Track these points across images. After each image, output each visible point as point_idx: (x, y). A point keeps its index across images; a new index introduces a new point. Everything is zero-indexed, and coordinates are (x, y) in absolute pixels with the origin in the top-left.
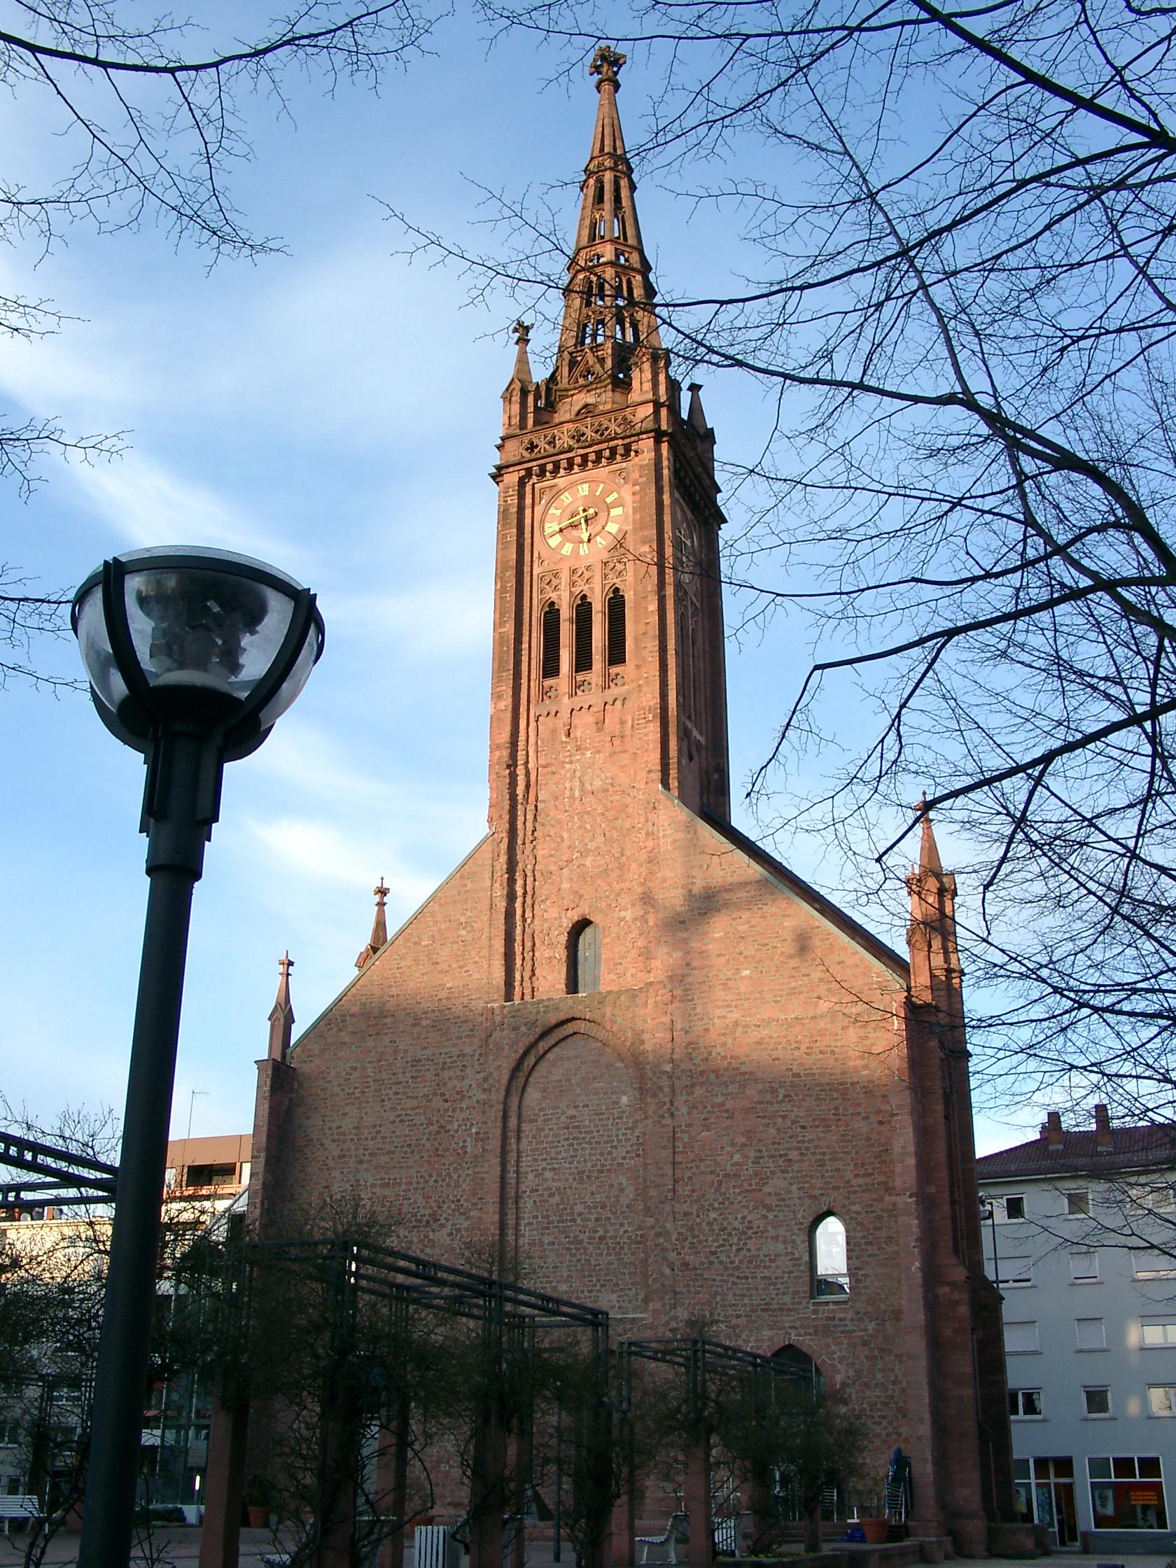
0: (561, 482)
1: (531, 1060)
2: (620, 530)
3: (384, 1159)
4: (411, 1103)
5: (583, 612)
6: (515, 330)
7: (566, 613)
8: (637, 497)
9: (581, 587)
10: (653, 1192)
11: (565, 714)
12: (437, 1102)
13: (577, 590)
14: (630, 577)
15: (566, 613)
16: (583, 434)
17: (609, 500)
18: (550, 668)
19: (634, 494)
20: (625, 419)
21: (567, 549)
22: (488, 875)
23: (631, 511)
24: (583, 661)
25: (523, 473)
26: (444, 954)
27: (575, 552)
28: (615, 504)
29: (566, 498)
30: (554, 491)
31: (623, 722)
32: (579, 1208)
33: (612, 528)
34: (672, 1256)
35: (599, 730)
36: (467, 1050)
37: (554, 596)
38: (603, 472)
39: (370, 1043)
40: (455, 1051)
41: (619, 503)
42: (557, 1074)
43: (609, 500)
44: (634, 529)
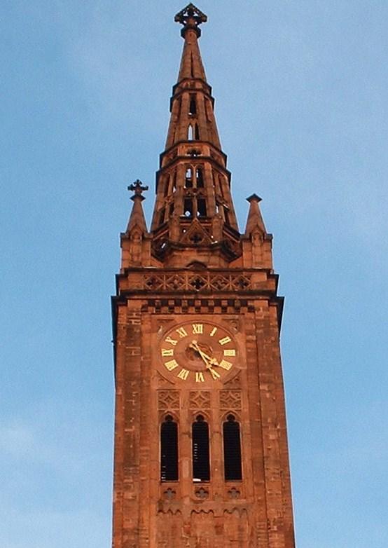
0: (178, 318)
2: (233, 369)
5: (200, 431)
6: (131, 188)
7: (185, 427)
8: (252, 345)
9: (200, 409)
11: (186, 513)
13: (196, 410)
14: (245, 407)
15: (185, 427)
16: (203, 284)
17: (223, 342)
18: (170, 470)
19: (248, 341)
20: (241, 280)
23: (244, 355)
24: (201, 469)
25: (146, 302)
27: (191, 379)
28: (227, 347)
29: (182, 332)
30: (171, 323)
31: (241, 530)
33: (226, 365)
35: (218, 533)
37: (172, 410)
38: (218, 319)
43: (223, 342)
44: (248, 372)
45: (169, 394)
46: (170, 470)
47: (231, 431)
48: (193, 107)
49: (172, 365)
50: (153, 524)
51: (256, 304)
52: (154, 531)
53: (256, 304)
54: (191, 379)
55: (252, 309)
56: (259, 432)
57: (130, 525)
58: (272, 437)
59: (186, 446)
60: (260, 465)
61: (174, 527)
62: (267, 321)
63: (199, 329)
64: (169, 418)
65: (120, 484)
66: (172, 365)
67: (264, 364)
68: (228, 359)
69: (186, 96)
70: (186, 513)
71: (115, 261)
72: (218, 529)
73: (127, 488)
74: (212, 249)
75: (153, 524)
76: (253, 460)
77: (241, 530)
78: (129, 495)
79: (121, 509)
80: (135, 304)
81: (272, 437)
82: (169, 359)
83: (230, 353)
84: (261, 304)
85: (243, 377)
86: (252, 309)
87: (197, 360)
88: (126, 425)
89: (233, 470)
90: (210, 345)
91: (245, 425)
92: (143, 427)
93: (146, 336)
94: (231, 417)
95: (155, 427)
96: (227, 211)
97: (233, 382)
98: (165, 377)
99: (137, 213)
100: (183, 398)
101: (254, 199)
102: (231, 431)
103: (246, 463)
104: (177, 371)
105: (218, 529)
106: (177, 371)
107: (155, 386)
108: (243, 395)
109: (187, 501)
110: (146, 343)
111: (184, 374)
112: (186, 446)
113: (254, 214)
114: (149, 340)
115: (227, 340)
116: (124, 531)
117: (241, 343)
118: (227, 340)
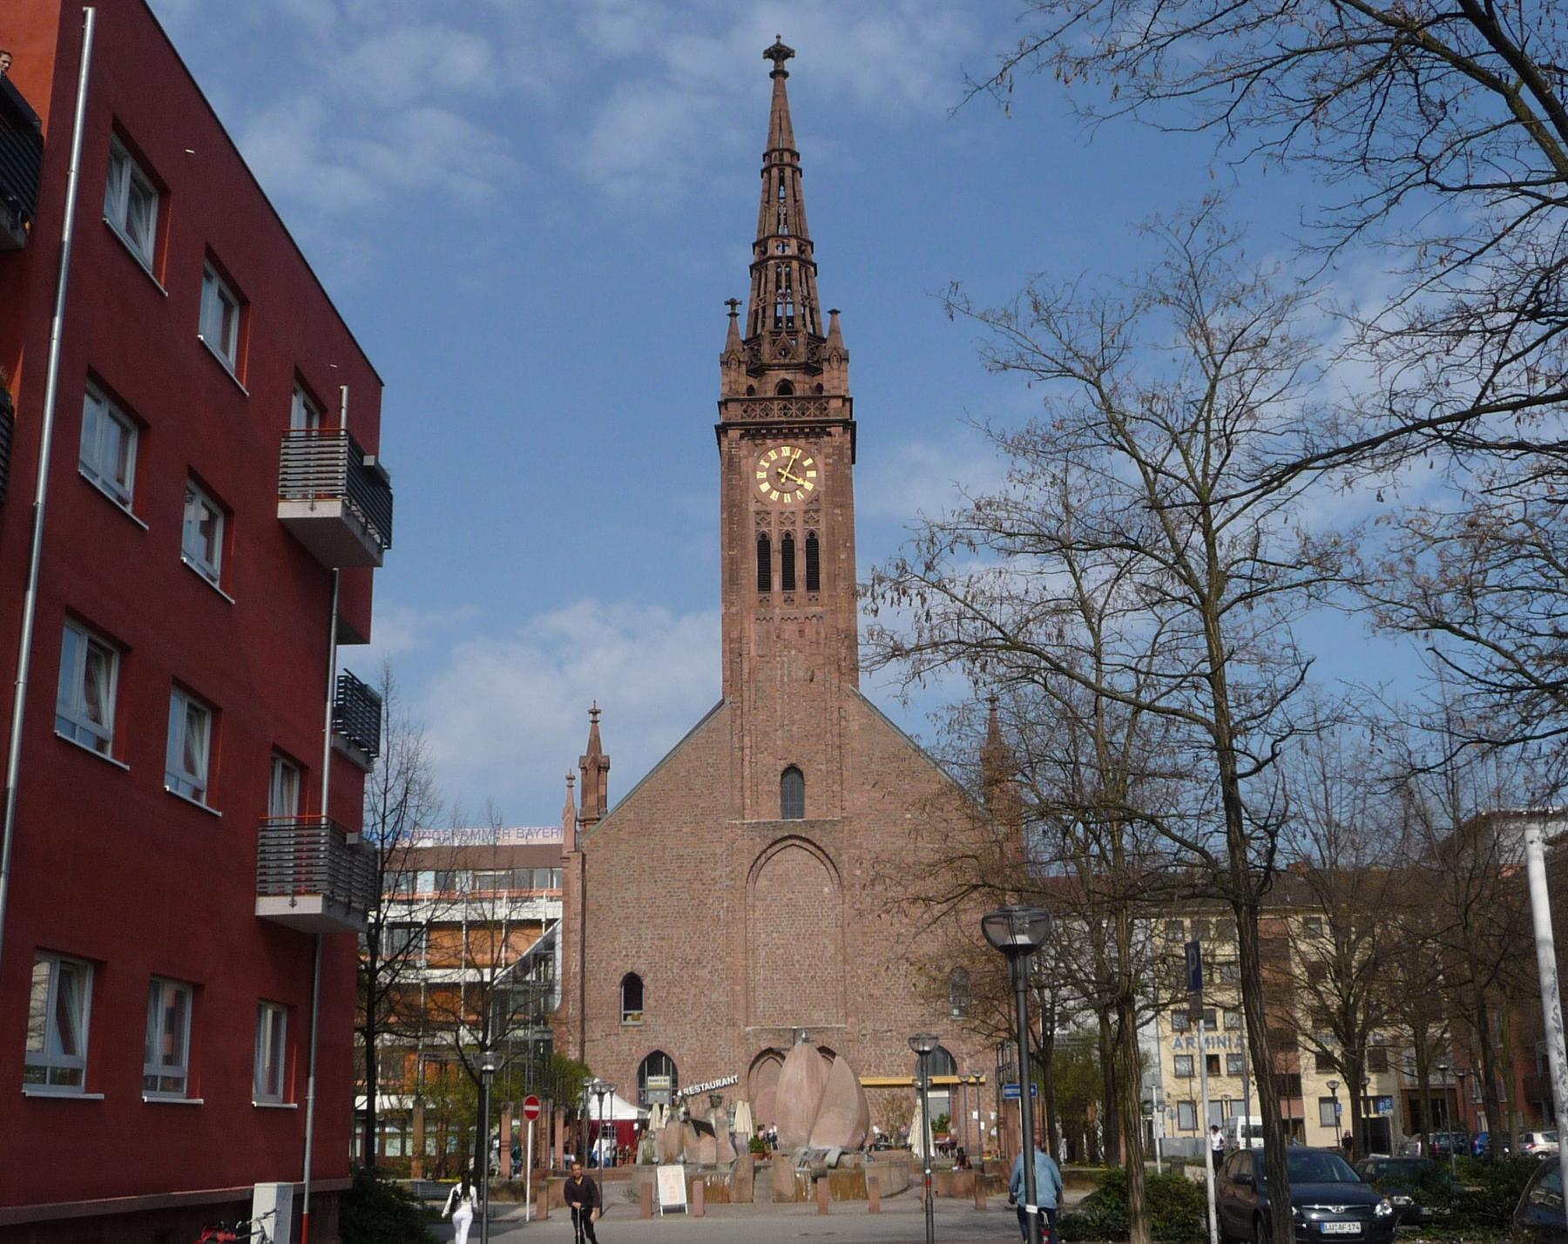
0: (769, 442)
1: (763, 859)
3: (660, 921)
4: (678, 884)
7: (776, 545)
10: (849, 950)
11: (777, 619)
12: (697, 885)
15: (776, 545)
18: (764, 584)
21: (775, 495)
22: (728, 732)
24: (789, 583)
26: (698, 784)
27: (781, 498)
28: (810, 468)
29: (773, 455)
31: (818, 633)
32: (797, 957)
33: (809, 486)
34: (862, 990)
36: (718, 851)
38: (802, 442)
39: (644, 841)
40: (709, 852)
41: (812, 467)
42: (780, 869)
44: (826, 493)
45: (763, 515)
46: (764, 584)
47: (812, 543)
48: (782, 181)
49: (765, 487)
50: (752, 630)
51: (833, 430)
52: (753, 635)
53: (833, 430)
54: (781, 498)
55: (829, 434)
56: (833, 549)
57: (735, 635)
58: (843, 557)
59: (776, 561)
60: (833, 578)
61: (768, 631)
62: (840, 448)
63: (786, 451)
64: (764, 535)
65: (728, 602)
66: (765, 487)
67: (838, 489)
68: (810, 480)
69: (775, 171)
70: (777, 619)
71: (715, 383)
72: (801, 632)
73: (732, 604)
74: (797, 367)
75: (752, 630)
76: (828, 574)
77: (818, 633)
78: (734, 610)
79: (729, 621)
80: (734, 434)
81: (843, 557)
82: (763, 481)
83: (812, 474)
84: (837, 430)
85: (822, 498)
86: (829, 434)
87: (785, 478)
88: (731, 548)
89: (813, 583)
90: (797, 469)
91: (823, 543)
92: (744, 548)
93: (744, 461)
94: (812, 534)
95: (752, 545)
96: (812, 310)
97: (814, 500)
98: (762, 499)
99: (732, 331)
100: (773, 518)
101: (834, 312)
102: (812, 543)
103: (823, 577)
104: (769, 492)
105: (801, 632)
106: (769, 492)
107: (753, 507)
108: (821, 515)
109: (777, 611)
110: (744, 468)
111: (775, 495)
112: (776, 561)
113: (834, 331)
114: (746, 465)
115: (809, 461)
116: (731, 641)
117: (821, 466)
118: (809, 461)
